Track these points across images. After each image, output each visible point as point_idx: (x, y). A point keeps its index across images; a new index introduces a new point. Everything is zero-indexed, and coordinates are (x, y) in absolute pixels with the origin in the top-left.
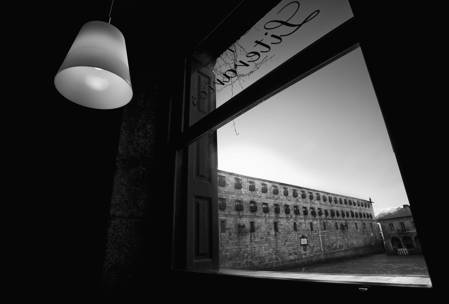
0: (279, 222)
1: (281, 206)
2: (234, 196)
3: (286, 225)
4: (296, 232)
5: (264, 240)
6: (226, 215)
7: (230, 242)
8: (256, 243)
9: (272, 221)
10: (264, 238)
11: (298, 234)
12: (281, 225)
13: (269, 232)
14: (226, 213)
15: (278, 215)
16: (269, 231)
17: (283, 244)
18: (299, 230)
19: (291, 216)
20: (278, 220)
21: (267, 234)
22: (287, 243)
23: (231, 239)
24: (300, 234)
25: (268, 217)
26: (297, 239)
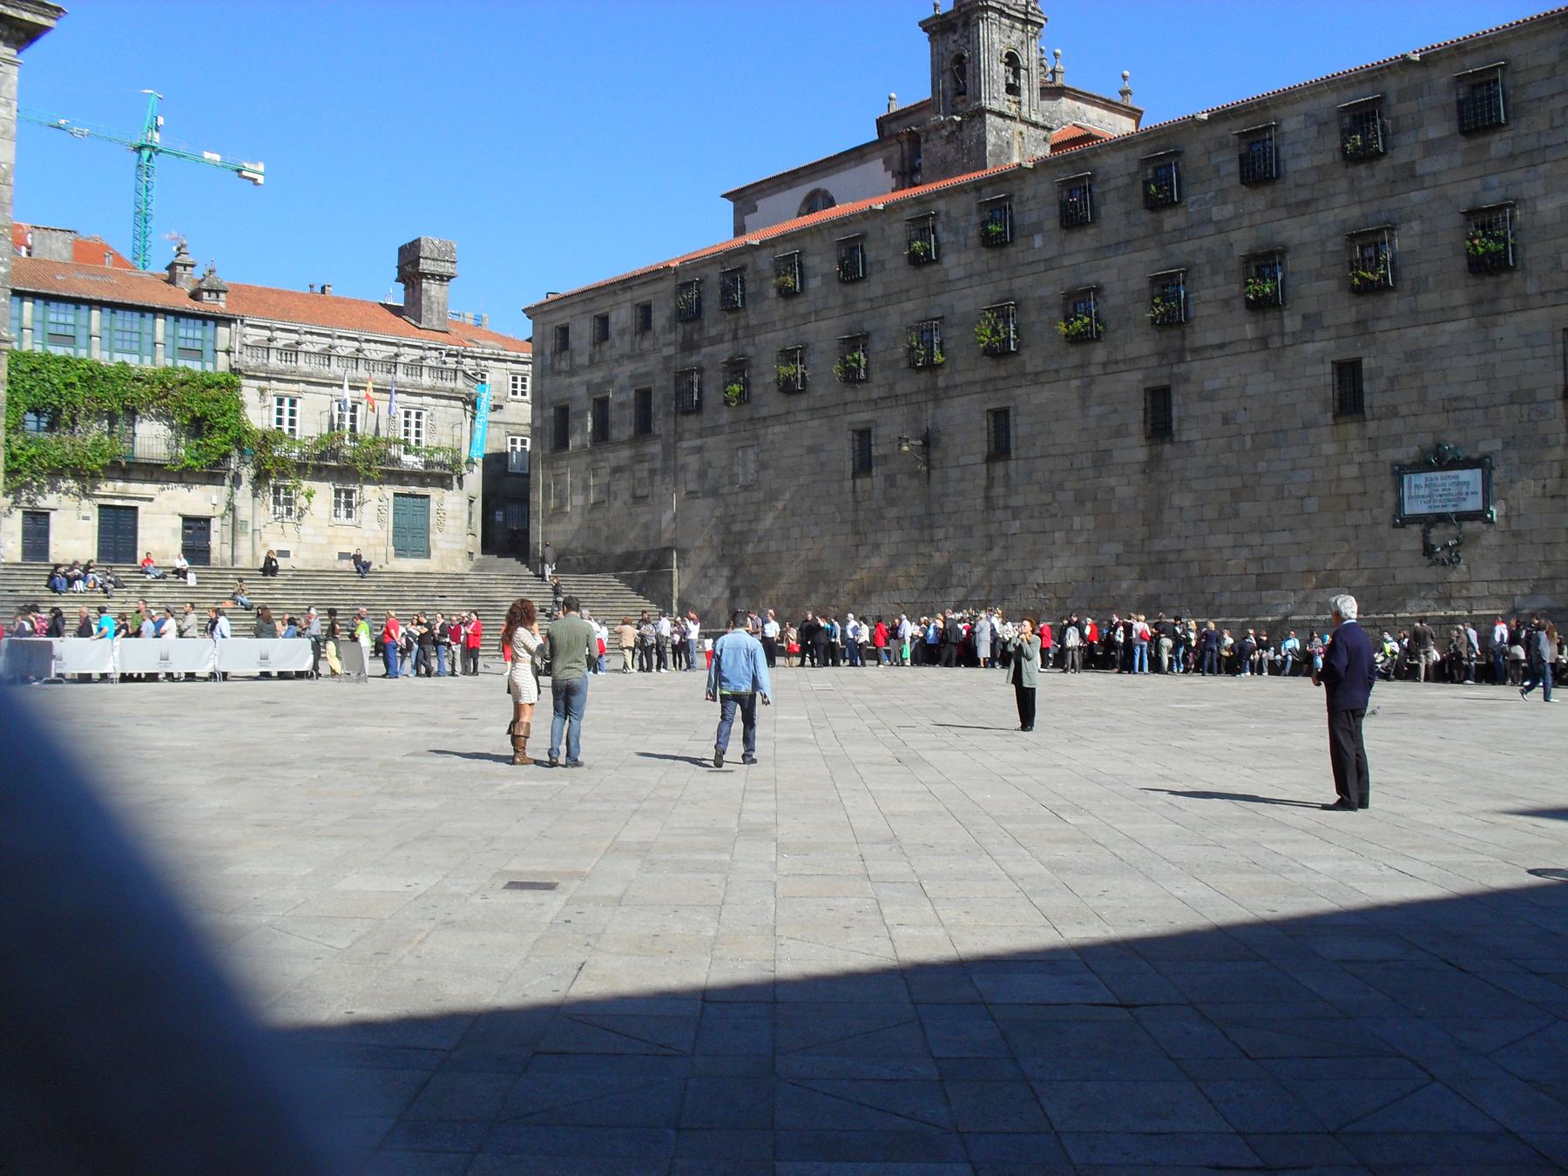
0: (1187, 380)
1: (1214, 272)
2: (908, 306)
3: (1250, 390)
4: (1352, 429)
5: (1067, 496)
6: (875, 402)
7: (892, 512)
8: (1013, 513)
9: (1130, 385)
10: (1068, 485)
11: (1373, 445)
12: (1210, 397)
13: (1108, 452)
14: (875, 394)
15: (1183, 336)
16: (1103, 445)
17: (1210, 512)
18: (1395, 407)
19: (1305, 317)
20: (1183, 367)
21: (1087, 463)
22: (1245, 507)
23: (892, 502)
24: (1397, 440)
25: (1104, 365)
26: (1362, 477)
